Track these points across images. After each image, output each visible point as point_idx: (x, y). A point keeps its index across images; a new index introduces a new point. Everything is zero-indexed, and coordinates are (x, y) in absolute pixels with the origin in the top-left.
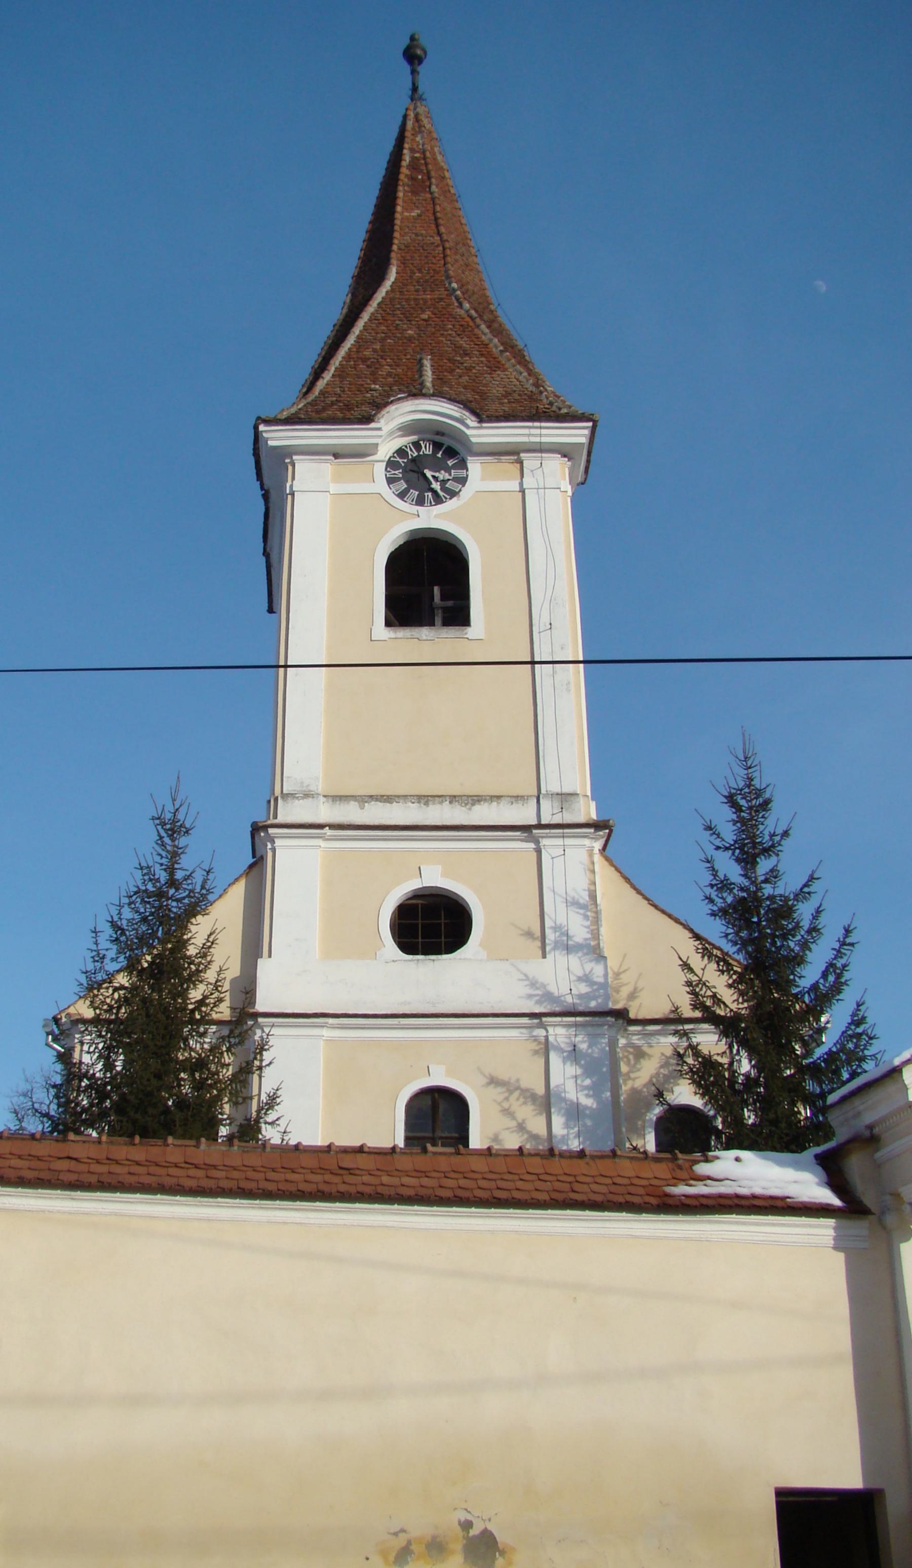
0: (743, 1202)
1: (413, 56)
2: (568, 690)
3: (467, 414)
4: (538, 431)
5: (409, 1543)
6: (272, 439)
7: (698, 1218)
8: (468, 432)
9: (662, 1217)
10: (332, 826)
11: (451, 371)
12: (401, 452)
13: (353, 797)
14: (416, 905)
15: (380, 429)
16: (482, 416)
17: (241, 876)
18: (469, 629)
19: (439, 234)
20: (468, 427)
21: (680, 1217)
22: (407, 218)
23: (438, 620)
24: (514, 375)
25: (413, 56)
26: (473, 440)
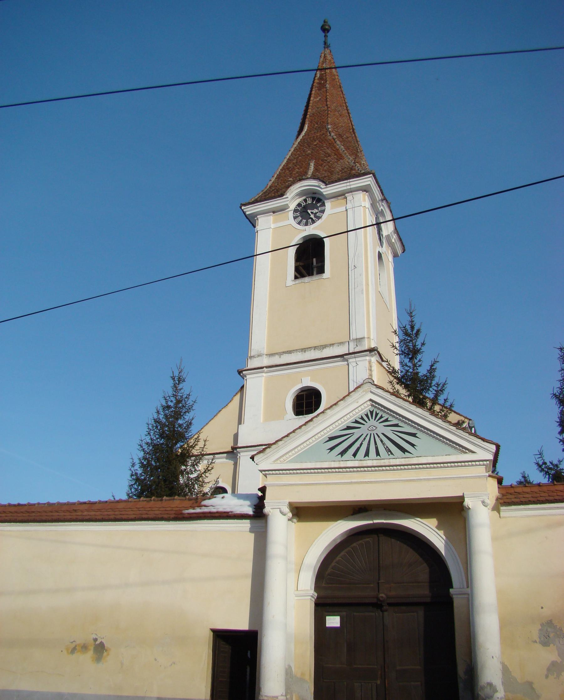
0: (213, 515)
1: (325, 29)
2: (362, 293)
3: (321, 183)
4: (348, 184)
5: (76, 646)
6: (248, 211)
7: (191, 522)
8: (322, 191)
9: (178, 522)
10: (267, 367)
11: (321, 165)
12: (299, 205)
14: (303, 395)
15: (287, 198)
16: (327, 182)
17: (238, 392)
18: (324, 274)
19: (327, 105)
20: (322, 188)
21: (184, 522)
22: (315, 102)
23: (315, 272)
25: (325, 29)
26: (324, 193)
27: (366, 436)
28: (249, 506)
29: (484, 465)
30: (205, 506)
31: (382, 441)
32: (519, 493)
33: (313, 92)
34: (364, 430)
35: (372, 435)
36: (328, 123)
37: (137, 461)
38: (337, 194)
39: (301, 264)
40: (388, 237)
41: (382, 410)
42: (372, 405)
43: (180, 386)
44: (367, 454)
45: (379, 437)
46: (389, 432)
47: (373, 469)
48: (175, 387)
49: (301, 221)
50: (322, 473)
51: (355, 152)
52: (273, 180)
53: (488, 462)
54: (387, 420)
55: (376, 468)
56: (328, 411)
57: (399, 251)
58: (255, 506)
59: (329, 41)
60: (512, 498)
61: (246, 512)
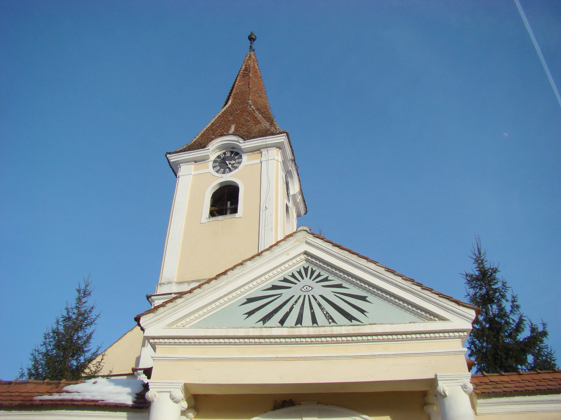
0: (75, 403)
1: (252, 39)
2: (272, 231)
4: (264, 140)
7: (43, 412)
8: (240, 145)
12: (219, 157)
13: (186, 282)
16: (246, 137)
18: (237, 214)
20: (240, 143)
21: (33, 412)
23: (228, 213)
24: (266, 124)
27: (298, 298)
28: (129, 394)
29: (460, 337)
30: (67, 392)
31: (320, 305)
32: (497, 383)
33: (238, 79)
34: (295, 290)
35: (307, 298)
36: (249, 100)
37: (26, 372)
38: (255, 149)
39: (216, 209)
40: (294, 196)
41: (320, 267)
42: (307, 260)
43: (84, 300)
44: (299, 321)
45: (316, 299)
46: (329, 293)
47: (308, 340)
48: (79, 299)
49: (219, 170)
50: (235, 344)
51: (271, 121)
52: (198, 137)
53: (465, 334)
54: (326, 279)
55: (313, 339)
56: (249, 262)
57: (303, 212)
58: (137, 394)
59: (254, 47)
60: (490, 388)
61: (122, 402)
